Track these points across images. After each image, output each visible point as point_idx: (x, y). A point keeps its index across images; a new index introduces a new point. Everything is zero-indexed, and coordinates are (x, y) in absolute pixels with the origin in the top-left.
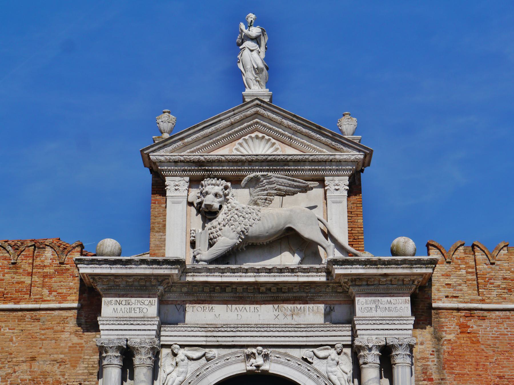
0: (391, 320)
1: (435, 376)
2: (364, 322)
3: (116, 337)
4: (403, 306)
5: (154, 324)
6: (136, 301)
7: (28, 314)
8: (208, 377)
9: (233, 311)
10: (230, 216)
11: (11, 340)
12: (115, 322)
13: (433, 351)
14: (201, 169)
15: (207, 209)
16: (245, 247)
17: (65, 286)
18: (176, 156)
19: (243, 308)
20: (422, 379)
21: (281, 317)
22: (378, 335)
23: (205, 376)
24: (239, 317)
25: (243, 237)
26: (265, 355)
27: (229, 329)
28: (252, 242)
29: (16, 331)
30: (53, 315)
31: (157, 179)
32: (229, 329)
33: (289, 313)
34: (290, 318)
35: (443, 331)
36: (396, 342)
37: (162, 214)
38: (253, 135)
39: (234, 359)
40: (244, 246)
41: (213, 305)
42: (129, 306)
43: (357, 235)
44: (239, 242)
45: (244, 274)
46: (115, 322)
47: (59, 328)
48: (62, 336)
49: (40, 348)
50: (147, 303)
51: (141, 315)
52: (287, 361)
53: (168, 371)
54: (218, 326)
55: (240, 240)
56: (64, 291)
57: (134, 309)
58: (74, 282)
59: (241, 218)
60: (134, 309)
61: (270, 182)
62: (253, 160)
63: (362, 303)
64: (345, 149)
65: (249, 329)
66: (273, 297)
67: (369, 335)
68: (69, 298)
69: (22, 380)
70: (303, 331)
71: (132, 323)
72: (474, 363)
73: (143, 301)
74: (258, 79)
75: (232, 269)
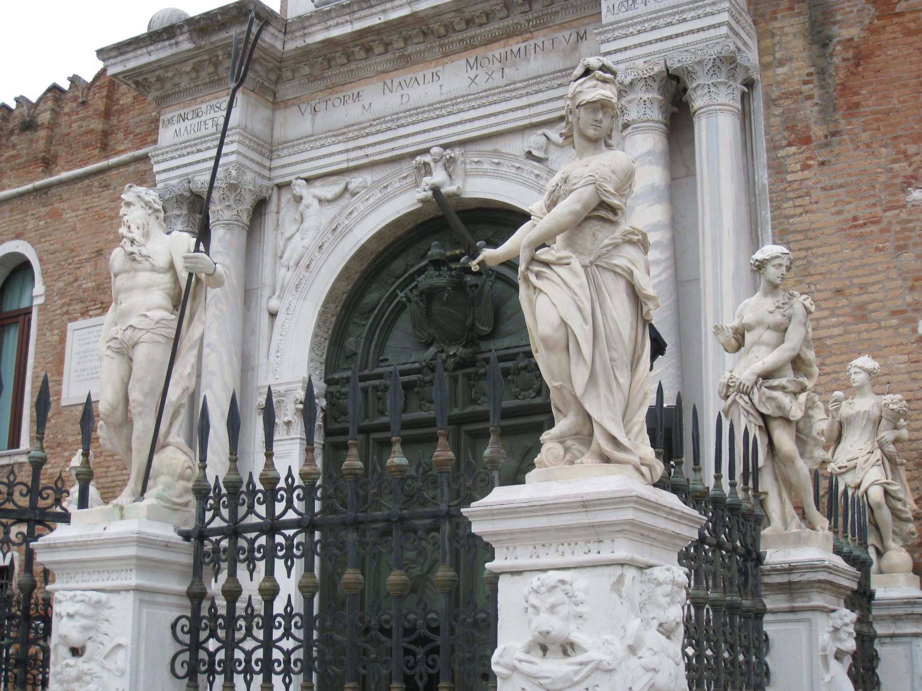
0: (677, 13)
1: (818, 131)
3: (177, 181)
7: (96, 181)
8: (355, 231)
11: (74, 229)
12: (174, 154)
13: (809, 75)
20: (784, 143)
21: (482, 77)
23: (348, 230)
24: (405, 98)
26: (448, 161)
27: (384, 126)
29: (80, 212)
32: (384, 126)
33: (497, 65)
34: (497, 75)
35: (835, 23)
36: (688, 59)
39: (397, 185)
41: (360, 89)
42: (198, 120)
49: (109, 233)
52: (494, 167)
53: (287, 235)
66: (462, 40)
69: (85, 291)
70: (522, 96)
72: (914, 81)
73: (218, 105)
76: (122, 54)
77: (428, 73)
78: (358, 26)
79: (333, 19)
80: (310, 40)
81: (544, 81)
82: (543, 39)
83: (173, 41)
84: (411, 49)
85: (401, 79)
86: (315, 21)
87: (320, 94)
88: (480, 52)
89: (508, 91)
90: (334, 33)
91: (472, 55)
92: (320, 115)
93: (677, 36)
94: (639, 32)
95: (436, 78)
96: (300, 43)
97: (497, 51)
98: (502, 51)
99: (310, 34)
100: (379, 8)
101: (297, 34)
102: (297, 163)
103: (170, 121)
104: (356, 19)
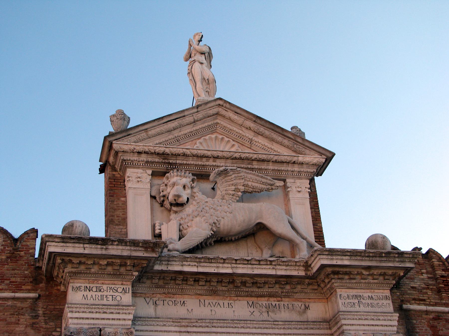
2: (349, 317)
3: (87, 326)
4: (385, 302)
5: (129, 313)
6: (109, 288)
9: (206, 306)
10: (201, 208)
12: (85, 310)
14: (164, 163)
15: (175, 200)
16: (214, 242)
17: (19, 274)
18: (140, 147)
19: (217, 304)
21: (257, 313)
22: (365, 330)
24: (213, 313)
25: (215, 229)
27: (204, 324)
28: (221, 236)
30: (6, 305)
31: (114, 173)
32: (204, 324)
33: (264, 309)
34: (265, 314)
37: (121, 207)
38: (213, 136)
40: (213, 240)
42: (99, 294)
43: (319, 238)
44: (211, 235)
45: (221, 265)
46: (85, 310)
47: (13, 320)
48: (17, 329)
50: (120, 290)
51: (115, 303)
54: (192, 321)
55: (213, 233)
56: (18, 280)
57: (106, 296)
58: (29, 270)
59: (212, 210)
60: (106, 296)
61: (238, 176)
62: (218, 156)
63: (345, 298)
64: (307, 151)
65: (225, 325)
66: (247, 292)
67: (355, 330)
68: (24, 287)
70: (281, 328)
71: (105, 311)
74: (208, 90)
75: (209, 259)
76: (63, 242)
77: (226, 302)
78: (201, 270)
79: (187, 261)
80: (171, 268)
81: (294, 324)
82: (287, 303)
83: (105, 247)
84: (220, 288)
85: (210, 301)
86: (177, 260)
87: (158, 295)
88: (254, 299)
89: (274, 324)
90: (186, 269)
91: (251, 300)
92: (159, 308)
93: (376, 325)
94: (359, 319)
95: (230, 306)
96: (164, 268)
97: (264, 302)
98: (266, 302)
99: (171, 265)
100: (215, 265)
101: (164, 263)
102: (147, 331)
103: (79, 288)
104: (200, 266)
